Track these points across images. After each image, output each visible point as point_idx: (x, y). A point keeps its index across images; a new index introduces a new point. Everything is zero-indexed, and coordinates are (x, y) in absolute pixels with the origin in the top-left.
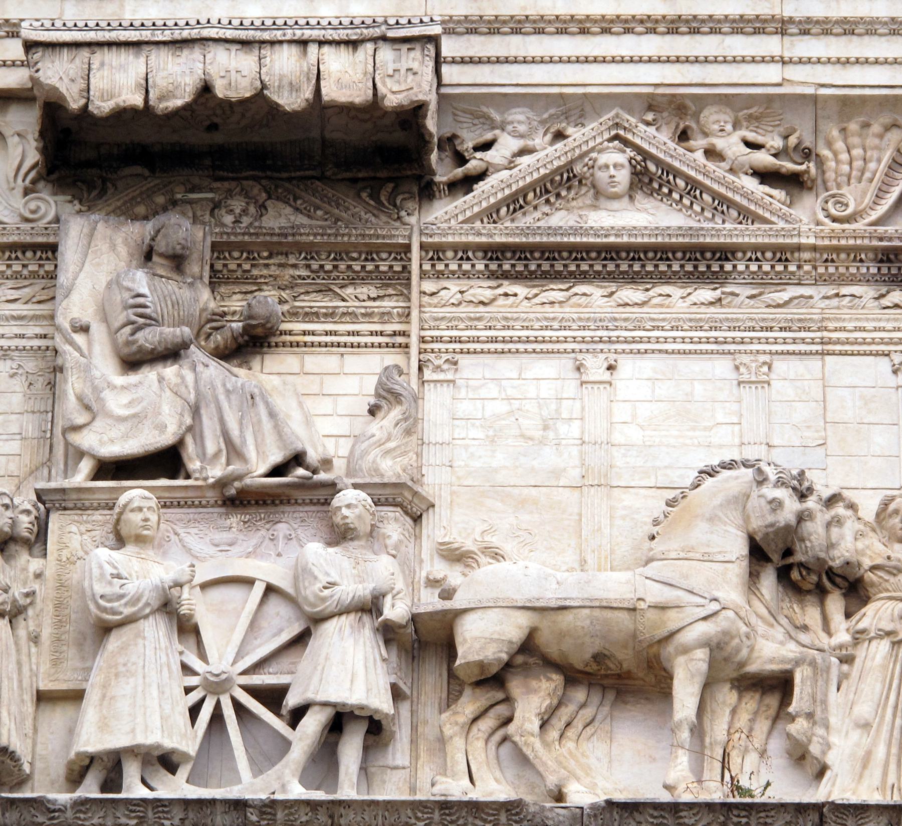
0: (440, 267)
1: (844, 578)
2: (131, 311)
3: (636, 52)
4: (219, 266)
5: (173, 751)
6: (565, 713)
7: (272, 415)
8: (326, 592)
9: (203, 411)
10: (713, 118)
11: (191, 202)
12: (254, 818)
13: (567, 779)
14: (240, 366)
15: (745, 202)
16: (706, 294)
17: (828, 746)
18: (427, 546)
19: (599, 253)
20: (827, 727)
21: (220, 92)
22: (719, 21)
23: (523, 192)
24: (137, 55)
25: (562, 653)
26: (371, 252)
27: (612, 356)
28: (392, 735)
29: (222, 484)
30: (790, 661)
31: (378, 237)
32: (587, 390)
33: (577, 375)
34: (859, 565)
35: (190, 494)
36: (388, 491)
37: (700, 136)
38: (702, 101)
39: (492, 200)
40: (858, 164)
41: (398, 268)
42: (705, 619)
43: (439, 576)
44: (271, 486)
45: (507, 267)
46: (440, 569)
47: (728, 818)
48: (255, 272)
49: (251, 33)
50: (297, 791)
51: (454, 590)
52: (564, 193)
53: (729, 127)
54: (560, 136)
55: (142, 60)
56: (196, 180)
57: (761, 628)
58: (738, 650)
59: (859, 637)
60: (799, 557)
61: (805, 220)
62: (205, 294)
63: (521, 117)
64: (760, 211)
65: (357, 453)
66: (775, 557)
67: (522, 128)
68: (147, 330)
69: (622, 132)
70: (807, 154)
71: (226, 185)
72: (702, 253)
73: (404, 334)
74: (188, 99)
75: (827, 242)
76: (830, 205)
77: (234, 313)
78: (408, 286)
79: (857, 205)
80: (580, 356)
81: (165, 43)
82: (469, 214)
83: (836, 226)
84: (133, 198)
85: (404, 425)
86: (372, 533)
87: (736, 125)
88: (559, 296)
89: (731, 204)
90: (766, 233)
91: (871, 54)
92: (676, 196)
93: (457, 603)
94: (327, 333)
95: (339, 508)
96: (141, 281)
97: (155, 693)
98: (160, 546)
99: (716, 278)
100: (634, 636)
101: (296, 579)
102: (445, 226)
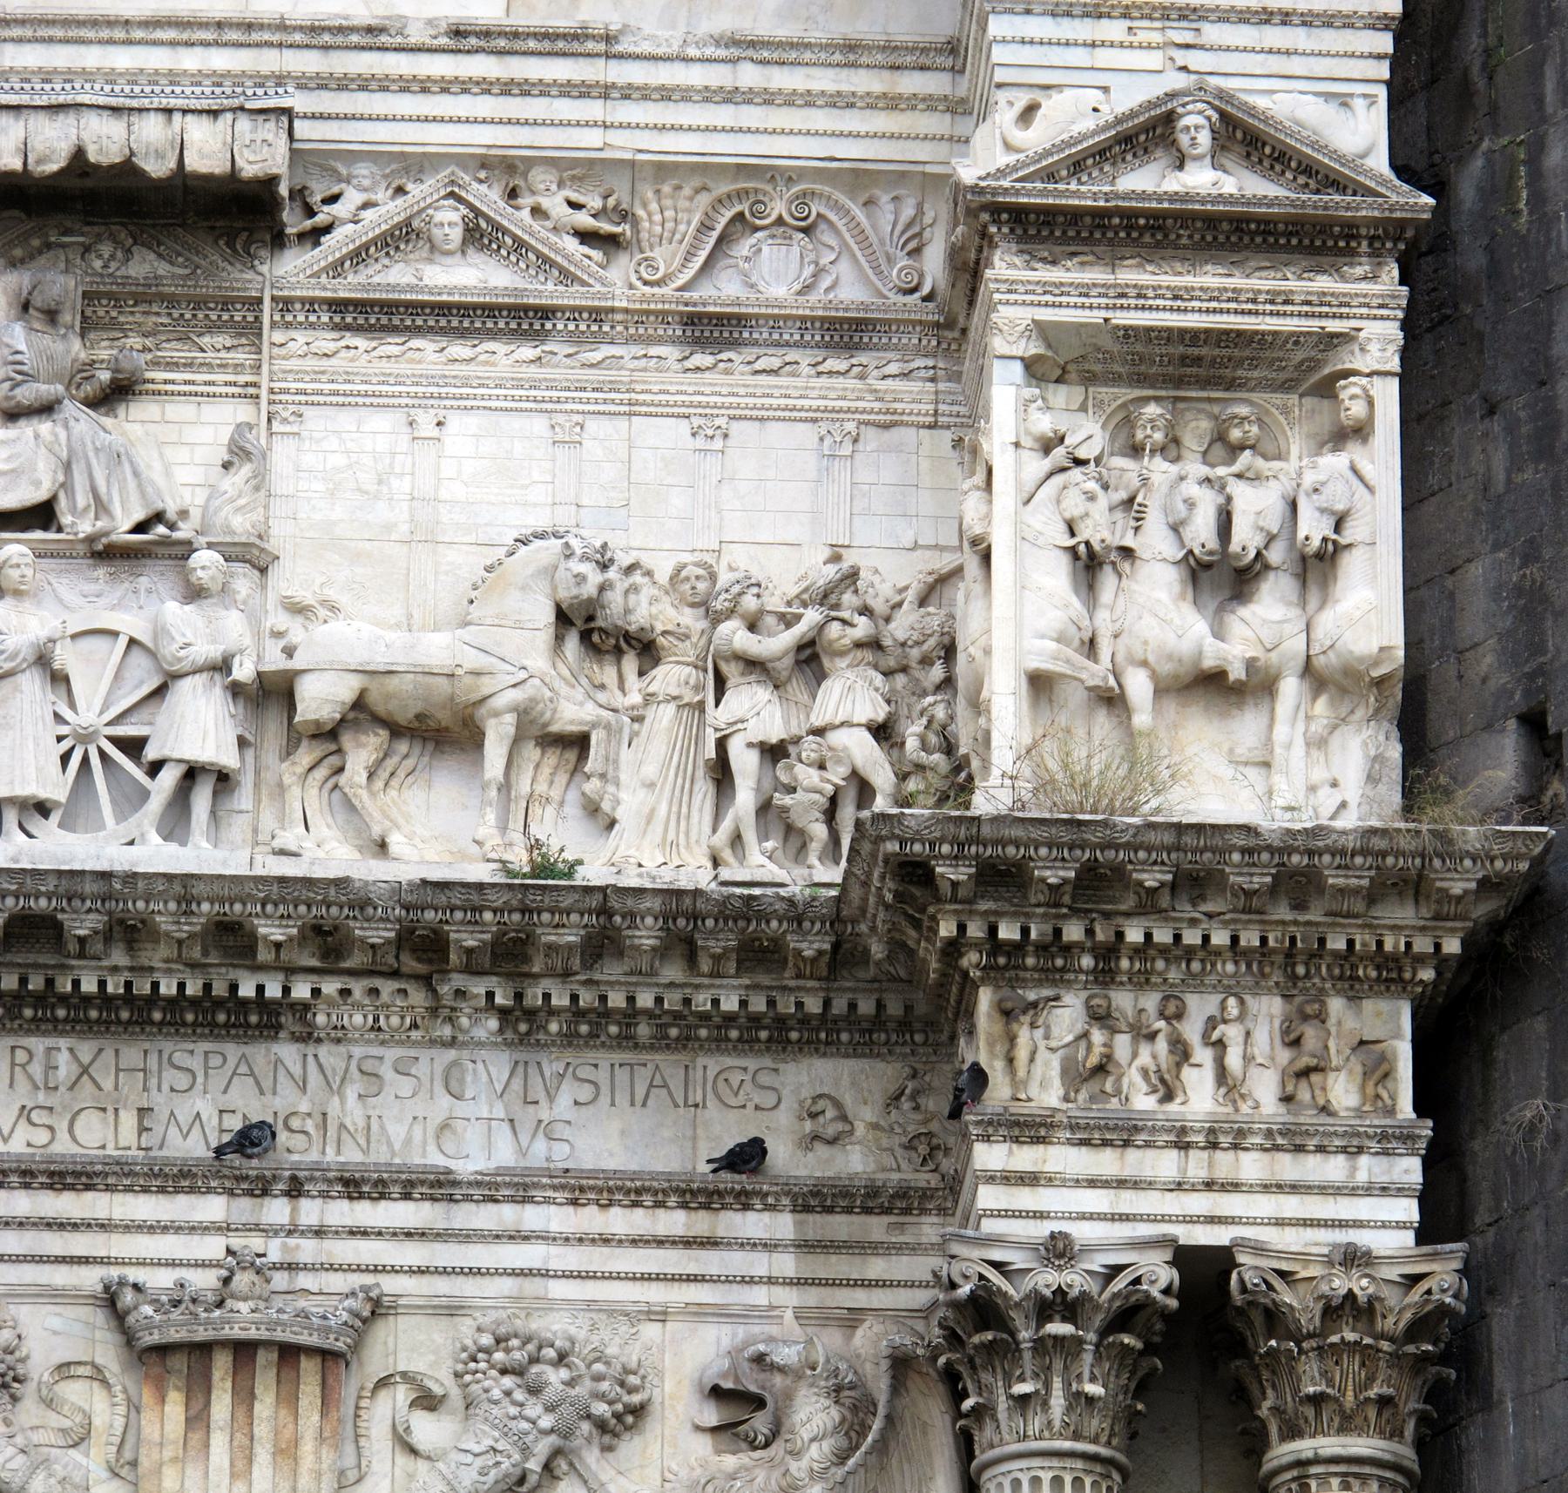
0: (289, 318)
1: (639, 641)
2: (10, 367)
3: (472, 114)
4: (88, 312)
5: (47, 800)
6: (390, 763)
7: (136, 474)
8: (182, 653)
9: (74, 467)
10: (541, 178)
11: (63, 246)
12: (118, 886)
13: (390, 829)
14: (107, 415)
15: (565, 264)
16: (527, 352)
17: (617, 802)
18: (272, 598)
19: (433, 309)
20: (618, 785)
21: (93, 157)
22: (548, 85)
23: (366, 246)
24: (17, 118)
25: (389, 713)
26: (226, 303)
27: (442, 412)
28: (238, 783)
29: (91, 540)
30: (587, 723)
31: (233, 289)
32: (418, 445)
33: (409, 430)
34: (652, 630)
35: (62, 546)
36: (238, 549)
37: (527, 193)
38: (530, 162)
39: (338, 255)
40: (670, 225)
41: (250, 319)
42: (514, 686)
43: (282, 629)
44: (135, 543)
45: (349, 320)
47: (525, 896)
48: (122, 319)
49: (122, 100)
51: (295, 648)
52: (402, 247)
53: (554, 187)
54: (400, 191)
55: (22, 123)
56: (68, 224)
57: (564, 689)
58: (542, 714)
59: (649, 698)
60: (599, 623)
61: (619, 284)
62: (76, 344)
63: (365, 172)
64: (579, 273)
65: (211, 509)
66: (579, 623)
67: (366, 183)
68: (25, 386)
69: (456, 190)
70: (624, 216)
71: (96, 229)
72: (526, 312)
73: (255, 385)
74: (63, 164)
75: (638, 306)
76: (642, 269)
77: (102, 361)
78: (260, 335)
79: (667, 268)
80: (412, 411)
81: (42, 107)
82: (316, 268)
83: (647, 289)
84: (12, 241)
85: (253, 482)
86: (224, 588)
87: (561, 185)
88: (395, 350)
89: (553, 264)
90: (584, 296)
91: (686, 122)
92: (504, 252)
93: (297, 663)
94: (186, 382)
95: (195, 569)
96: (18, 337)
97: (31, 746)
98: (35, 595)
99: (539, 336)
100: (452, 699)
101: (155, 638)
102: (294, 279)
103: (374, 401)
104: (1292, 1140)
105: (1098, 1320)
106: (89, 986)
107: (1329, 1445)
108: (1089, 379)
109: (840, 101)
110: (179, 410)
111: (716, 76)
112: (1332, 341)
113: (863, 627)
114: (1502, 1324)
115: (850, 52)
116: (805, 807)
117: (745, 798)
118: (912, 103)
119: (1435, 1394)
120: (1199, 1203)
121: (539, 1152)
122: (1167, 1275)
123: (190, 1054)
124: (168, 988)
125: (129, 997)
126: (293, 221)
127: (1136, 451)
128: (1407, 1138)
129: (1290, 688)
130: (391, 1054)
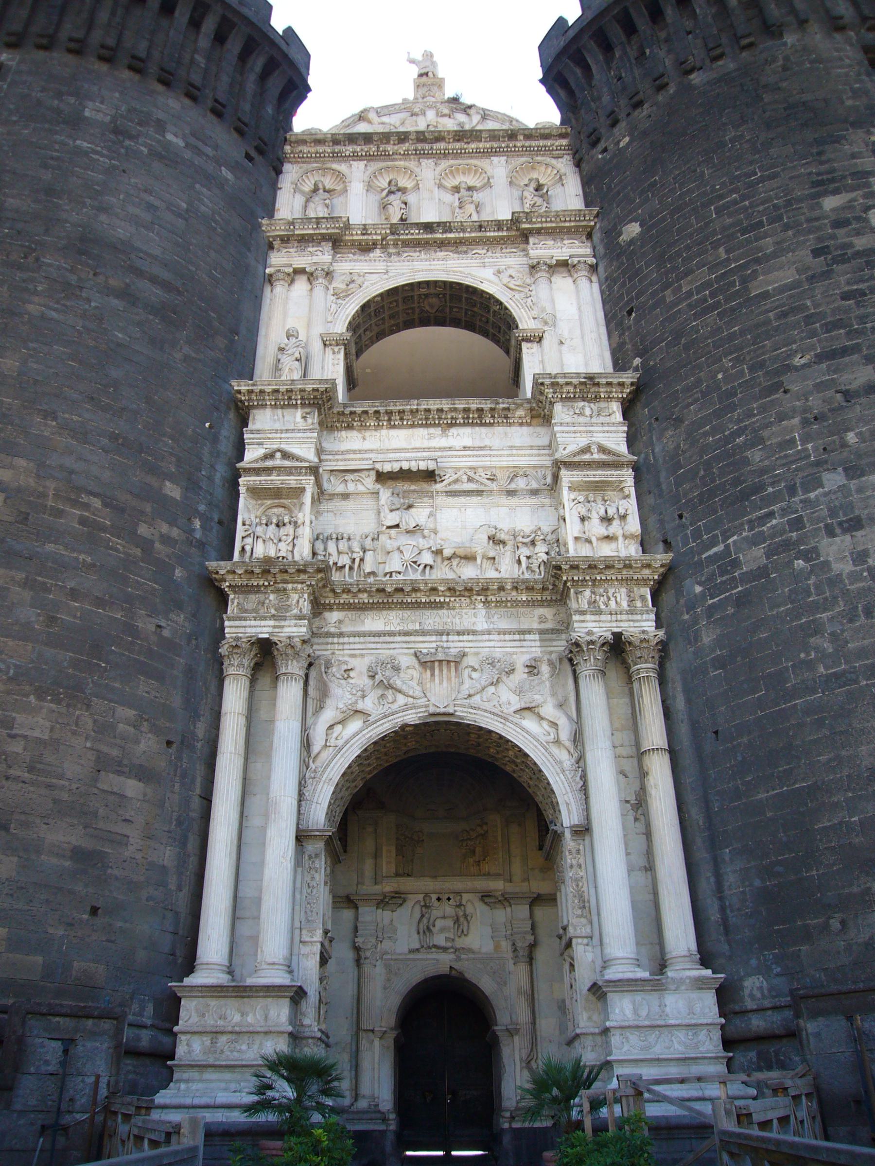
10: (480, 470)
46: (440, 542)
50: (420, 578)
99: (481, 496)
103: (454, 507)
104: (631, 612)
105: (598, 645)
106: (409, 601)
107: (643, 666)
108: (580, 491)
109: (529, 455)
110: (420, 510)
111: (509, 452)
112: (621, 482)
113: (542, 537)
114: (672, 646)
115: (532, 448)
116: (535, 566)
117: (524, 565)
118: (543, 455)
119: (661, 657)
120: (614, 624)
121: (492, 626)
122: (611, 636)
123: (428, 613)
124: (423, 600)
125: (416, 602)
126: (438, 479)
127: (589, 502)
128: (652, 611)
129: (621, 539)
130: (464, 611)
